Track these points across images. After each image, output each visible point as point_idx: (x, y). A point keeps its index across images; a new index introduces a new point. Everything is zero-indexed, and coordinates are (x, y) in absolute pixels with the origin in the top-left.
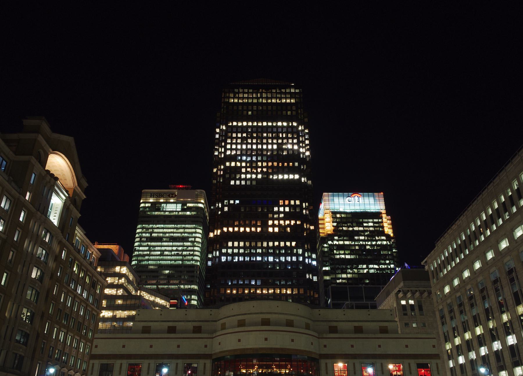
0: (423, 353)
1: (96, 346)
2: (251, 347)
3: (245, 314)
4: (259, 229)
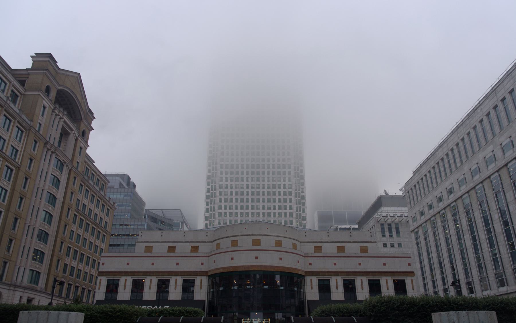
0: (399, 270)
1: (103, 264)
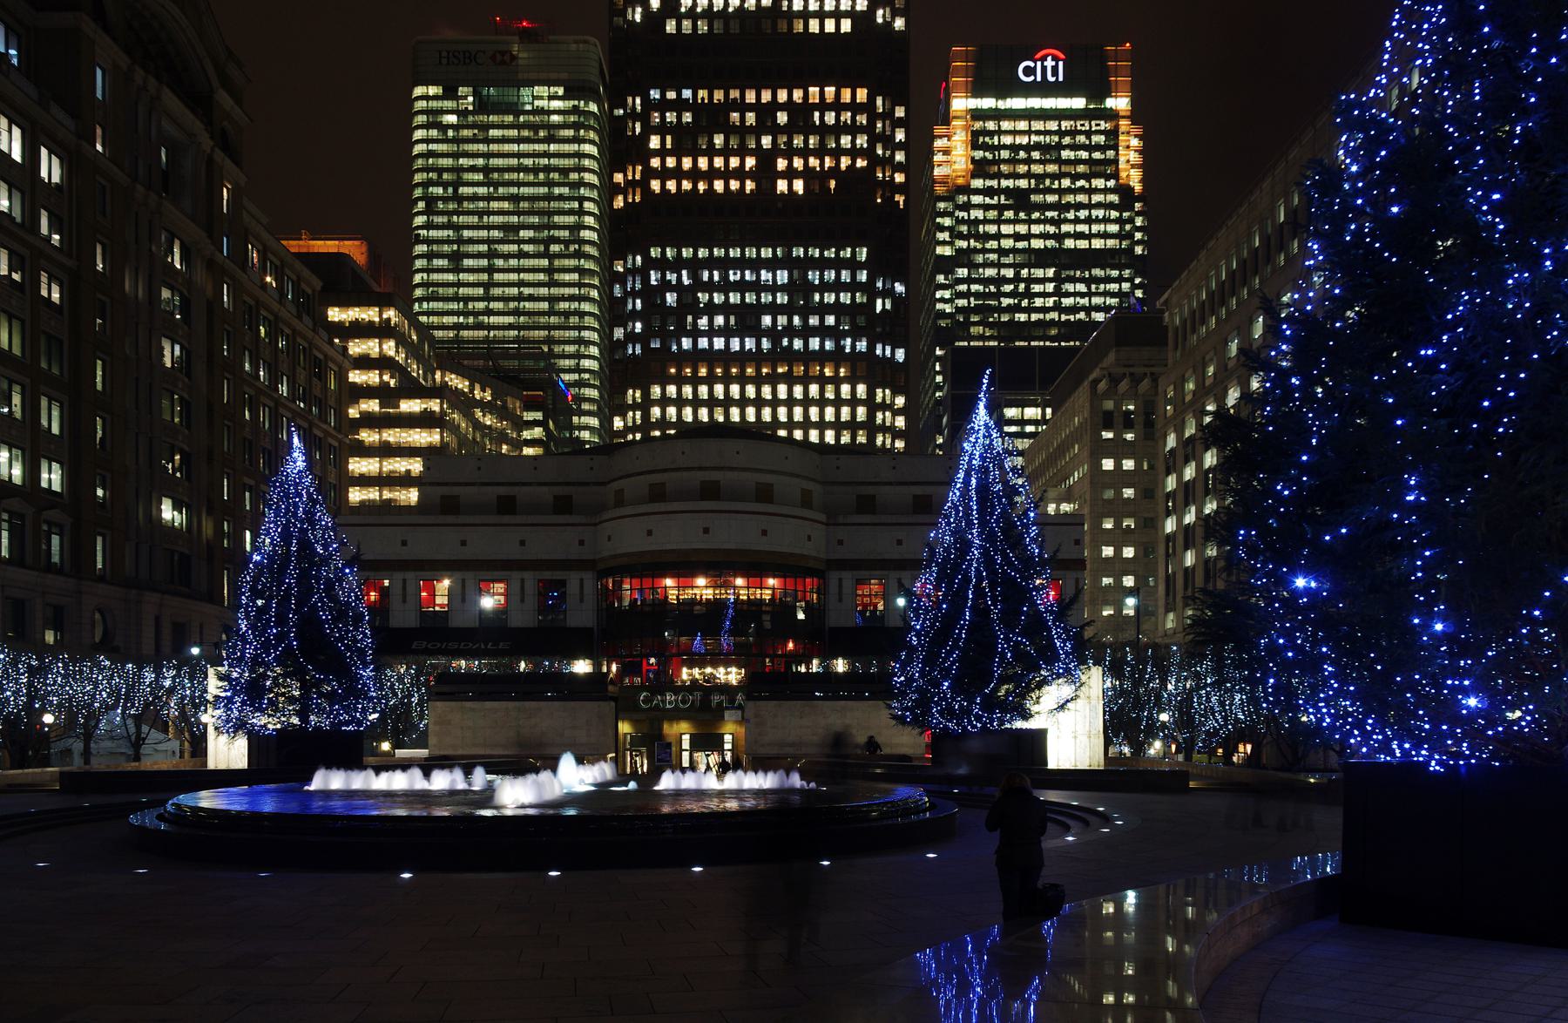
2: (674, 547)
3: (665, 471)
4: (750, 185)
